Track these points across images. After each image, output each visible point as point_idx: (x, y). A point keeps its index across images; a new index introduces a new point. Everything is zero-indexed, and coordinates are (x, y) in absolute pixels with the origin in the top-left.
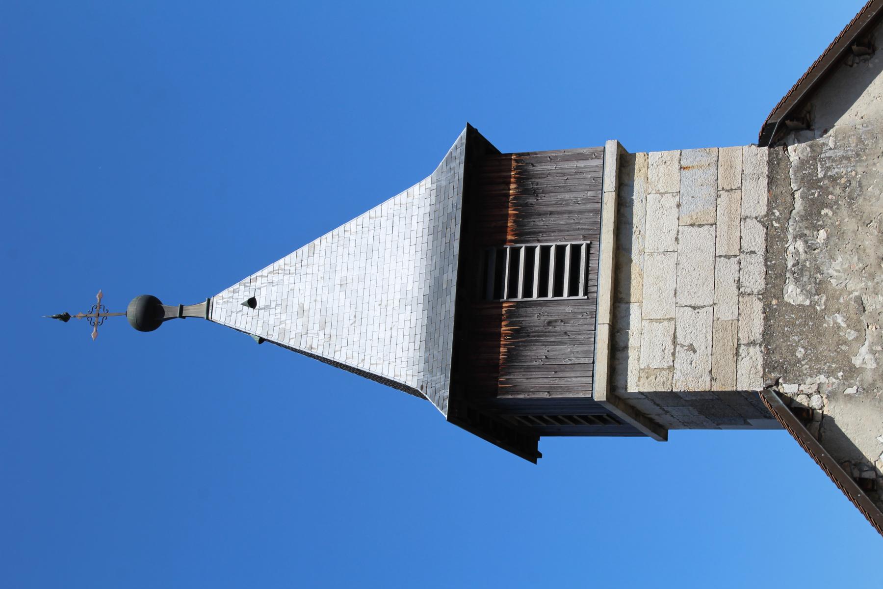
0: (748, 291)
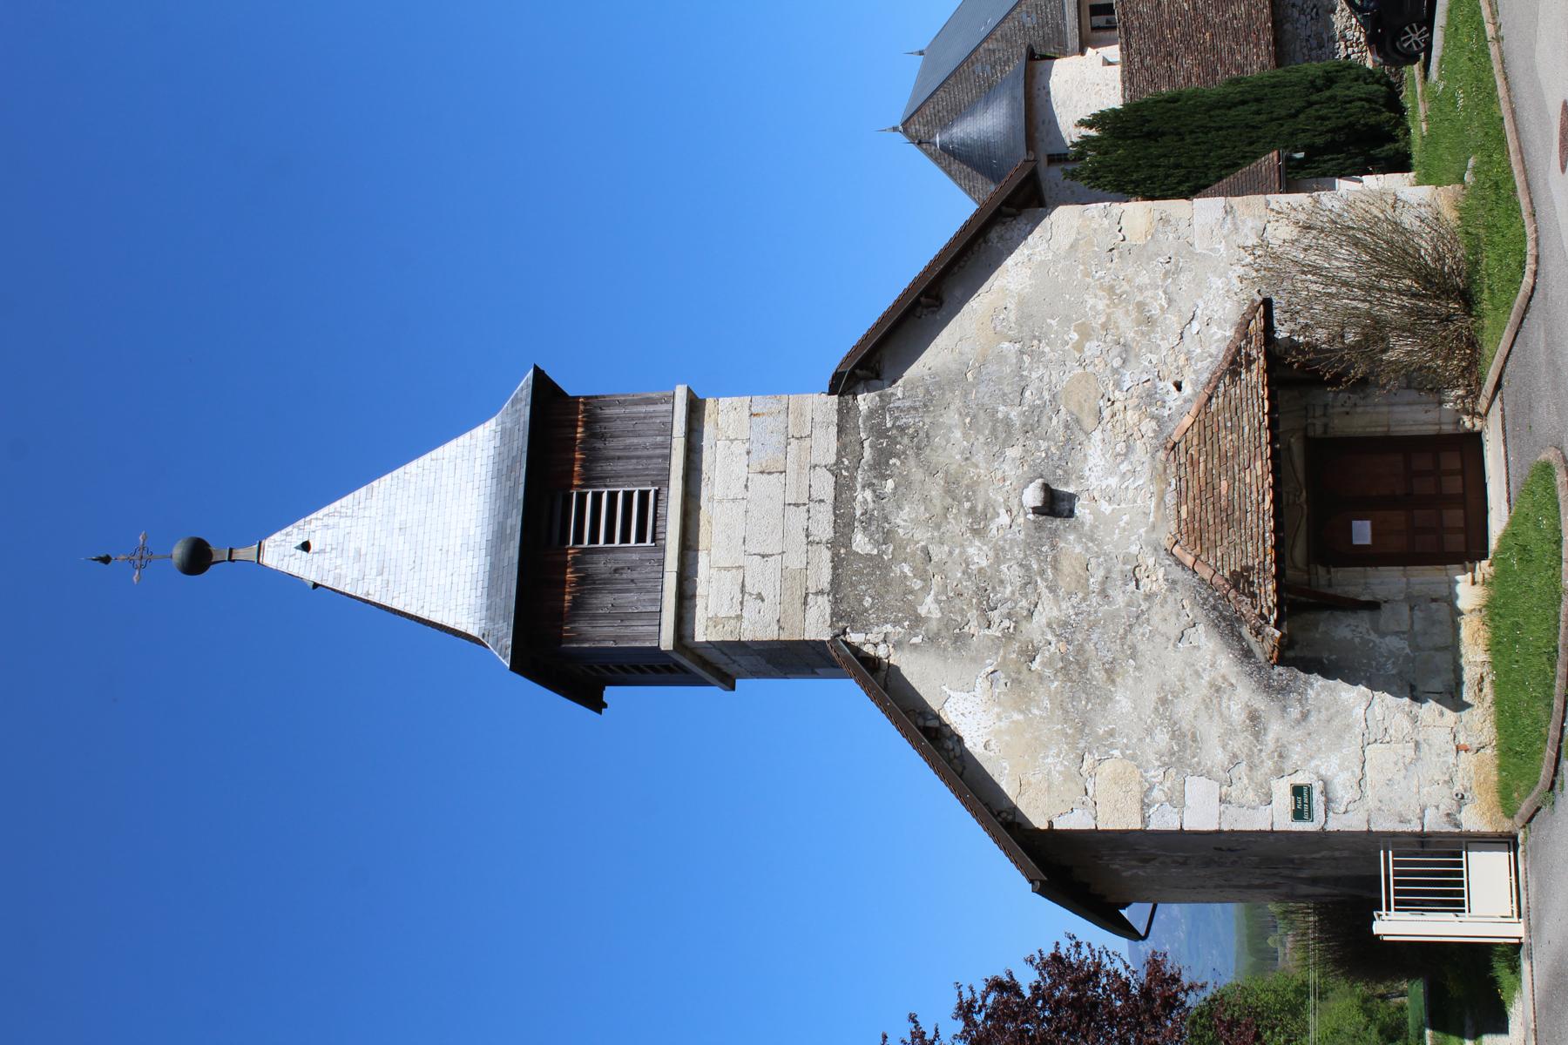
0: (817, 539)
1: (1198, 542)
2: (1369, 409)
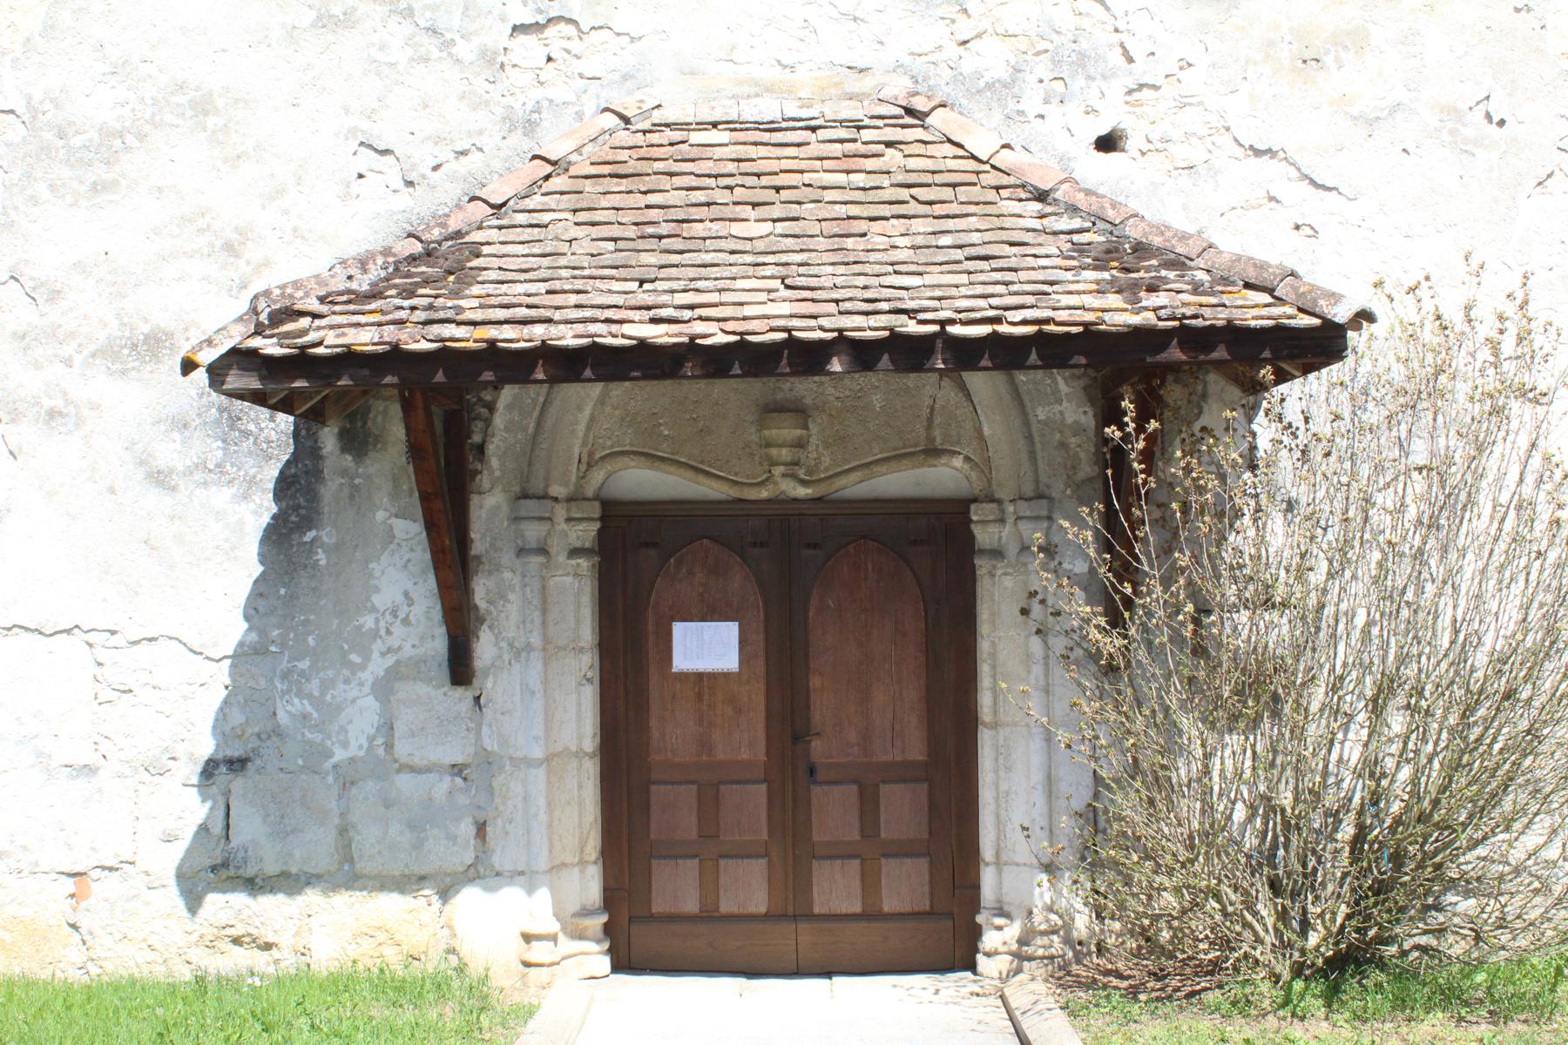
1: (606, 169)
2: (1037, 670)
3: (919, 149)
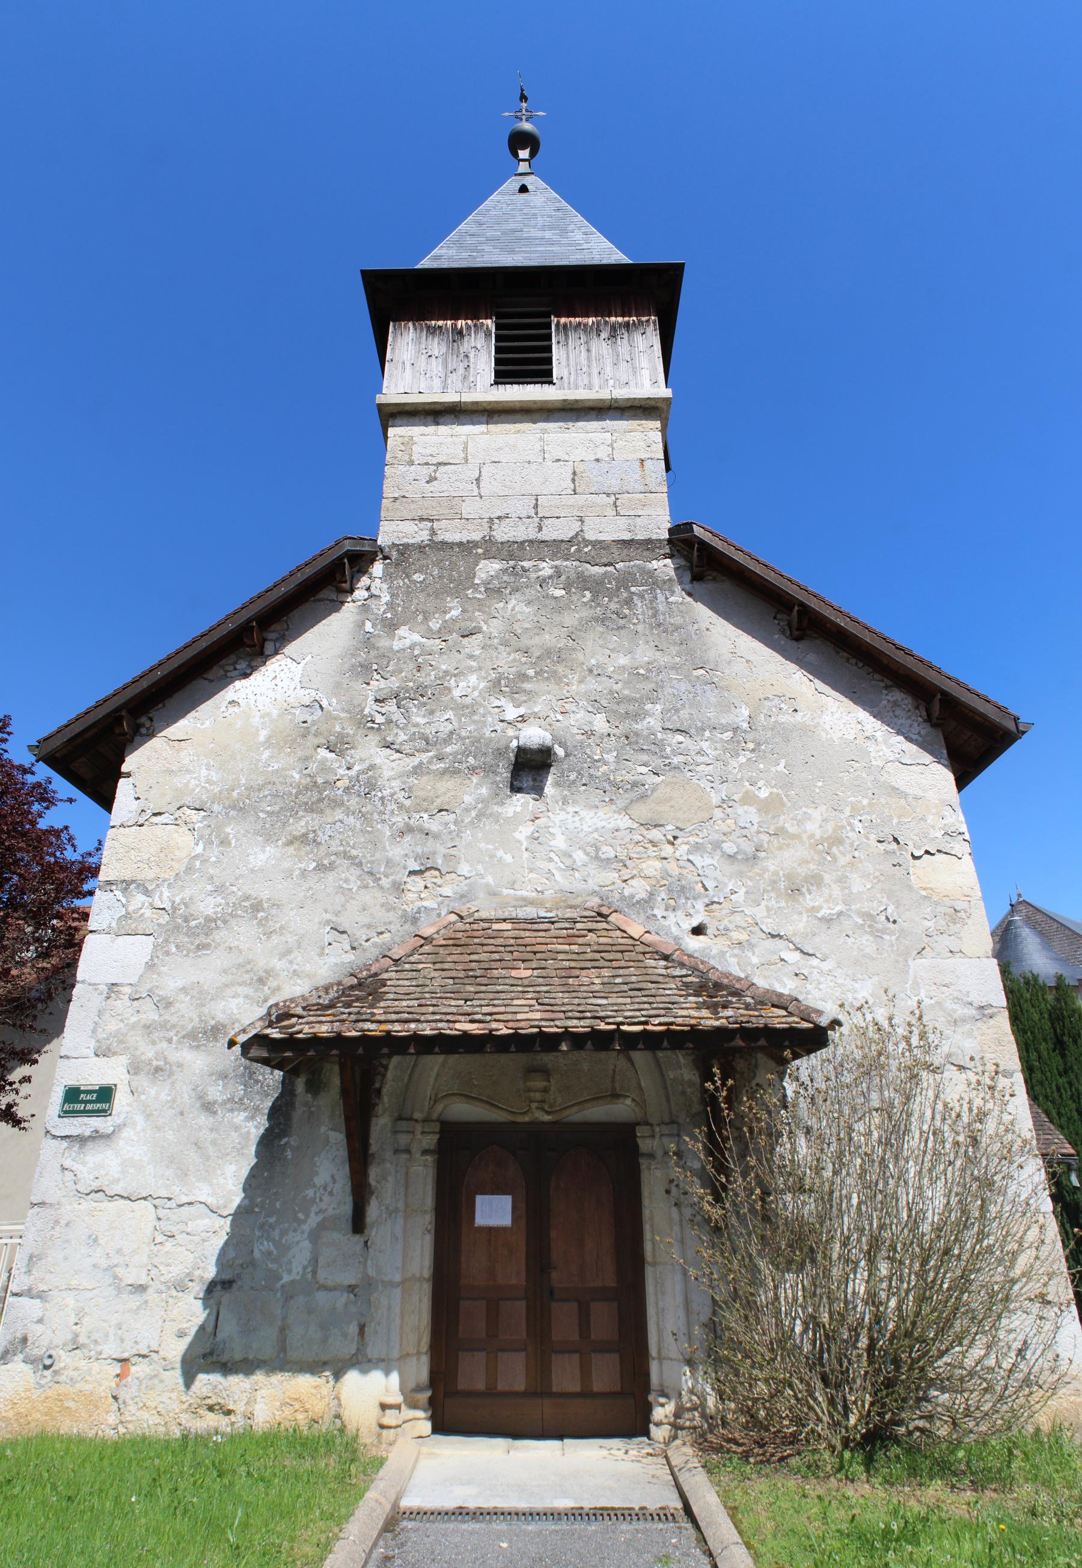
0: (495, 527)
1: (451, 942)
3: (604, 933)
